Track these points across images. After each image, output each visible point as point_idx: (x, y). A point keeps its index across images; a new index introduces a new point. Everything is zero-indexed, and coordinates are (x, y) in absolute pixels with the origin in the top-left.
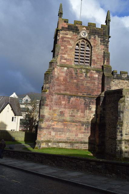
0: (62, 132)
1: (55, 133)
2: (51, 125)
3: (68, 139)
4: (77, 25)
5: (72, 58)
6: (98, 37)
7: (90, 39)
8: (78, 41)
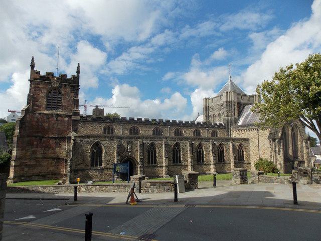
1: (27, 169)
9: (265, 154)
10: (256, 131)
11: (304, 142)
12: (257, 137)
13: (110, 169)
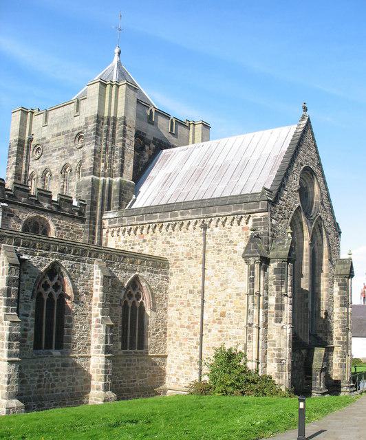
9: (226, 320)
10: (199, 231)
11: (336, 284)
12: (200, 253)
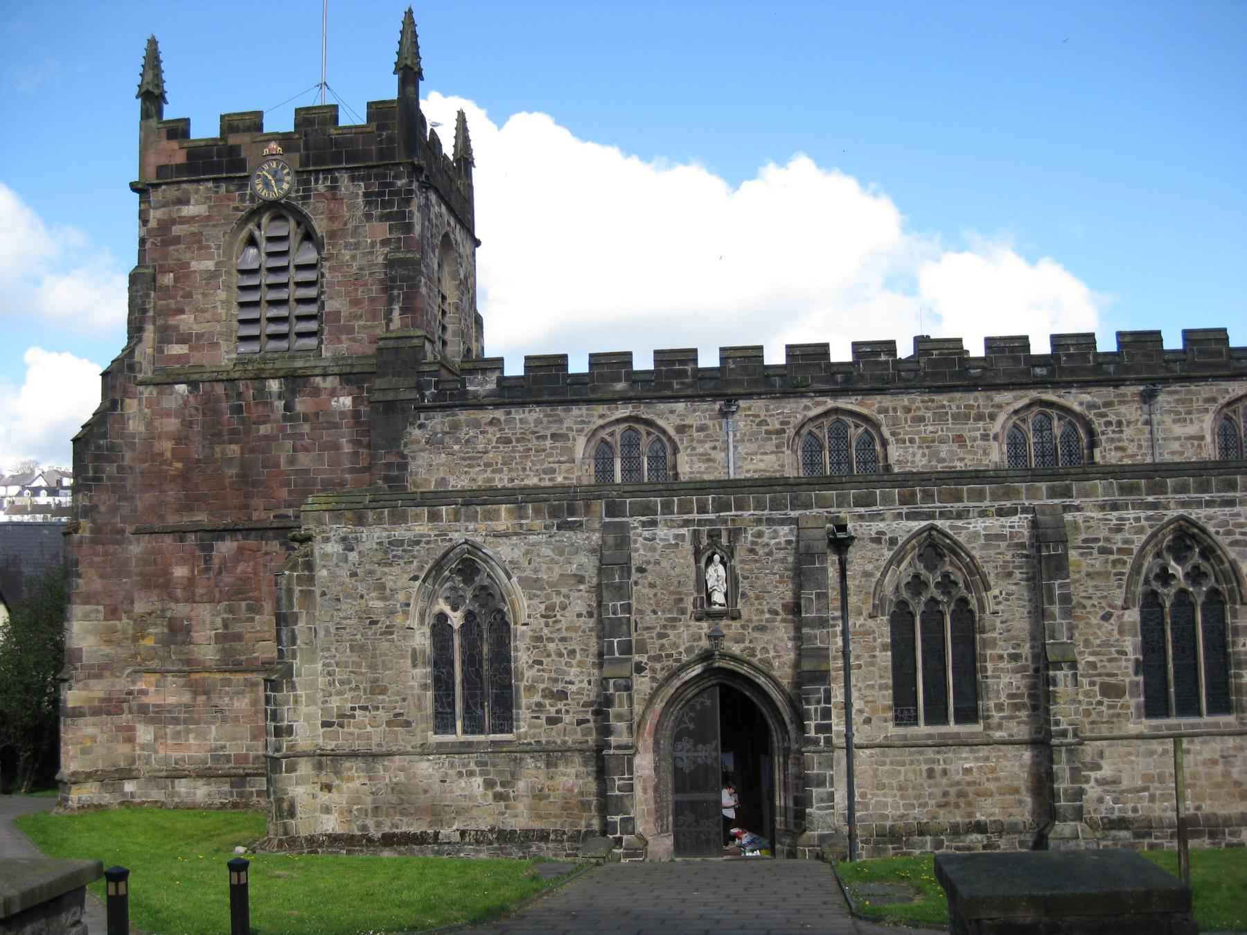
0: (186, 722)
1: (151, 729)
2: (130, 693)
3: (216, 758)
4: (233, 140)
5: (218, 327)
6: (353, 179)
7: (306, 198)
8: (251, 226)
13: (564, 751)
